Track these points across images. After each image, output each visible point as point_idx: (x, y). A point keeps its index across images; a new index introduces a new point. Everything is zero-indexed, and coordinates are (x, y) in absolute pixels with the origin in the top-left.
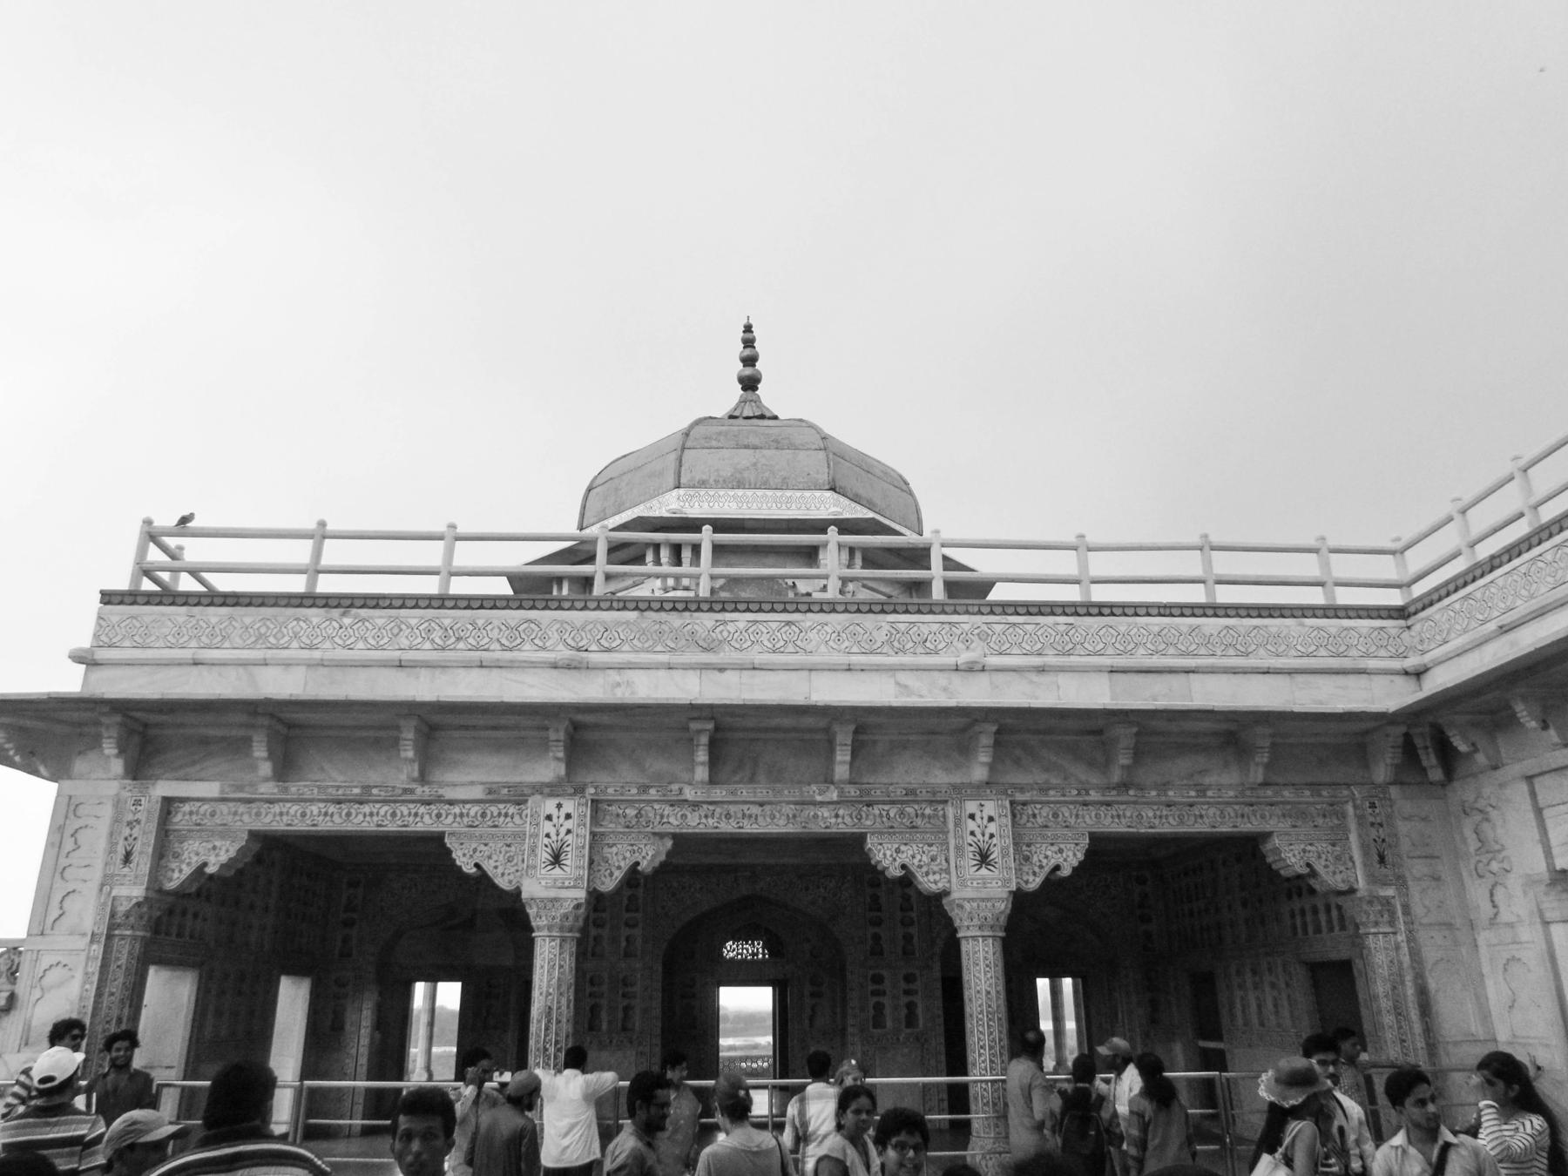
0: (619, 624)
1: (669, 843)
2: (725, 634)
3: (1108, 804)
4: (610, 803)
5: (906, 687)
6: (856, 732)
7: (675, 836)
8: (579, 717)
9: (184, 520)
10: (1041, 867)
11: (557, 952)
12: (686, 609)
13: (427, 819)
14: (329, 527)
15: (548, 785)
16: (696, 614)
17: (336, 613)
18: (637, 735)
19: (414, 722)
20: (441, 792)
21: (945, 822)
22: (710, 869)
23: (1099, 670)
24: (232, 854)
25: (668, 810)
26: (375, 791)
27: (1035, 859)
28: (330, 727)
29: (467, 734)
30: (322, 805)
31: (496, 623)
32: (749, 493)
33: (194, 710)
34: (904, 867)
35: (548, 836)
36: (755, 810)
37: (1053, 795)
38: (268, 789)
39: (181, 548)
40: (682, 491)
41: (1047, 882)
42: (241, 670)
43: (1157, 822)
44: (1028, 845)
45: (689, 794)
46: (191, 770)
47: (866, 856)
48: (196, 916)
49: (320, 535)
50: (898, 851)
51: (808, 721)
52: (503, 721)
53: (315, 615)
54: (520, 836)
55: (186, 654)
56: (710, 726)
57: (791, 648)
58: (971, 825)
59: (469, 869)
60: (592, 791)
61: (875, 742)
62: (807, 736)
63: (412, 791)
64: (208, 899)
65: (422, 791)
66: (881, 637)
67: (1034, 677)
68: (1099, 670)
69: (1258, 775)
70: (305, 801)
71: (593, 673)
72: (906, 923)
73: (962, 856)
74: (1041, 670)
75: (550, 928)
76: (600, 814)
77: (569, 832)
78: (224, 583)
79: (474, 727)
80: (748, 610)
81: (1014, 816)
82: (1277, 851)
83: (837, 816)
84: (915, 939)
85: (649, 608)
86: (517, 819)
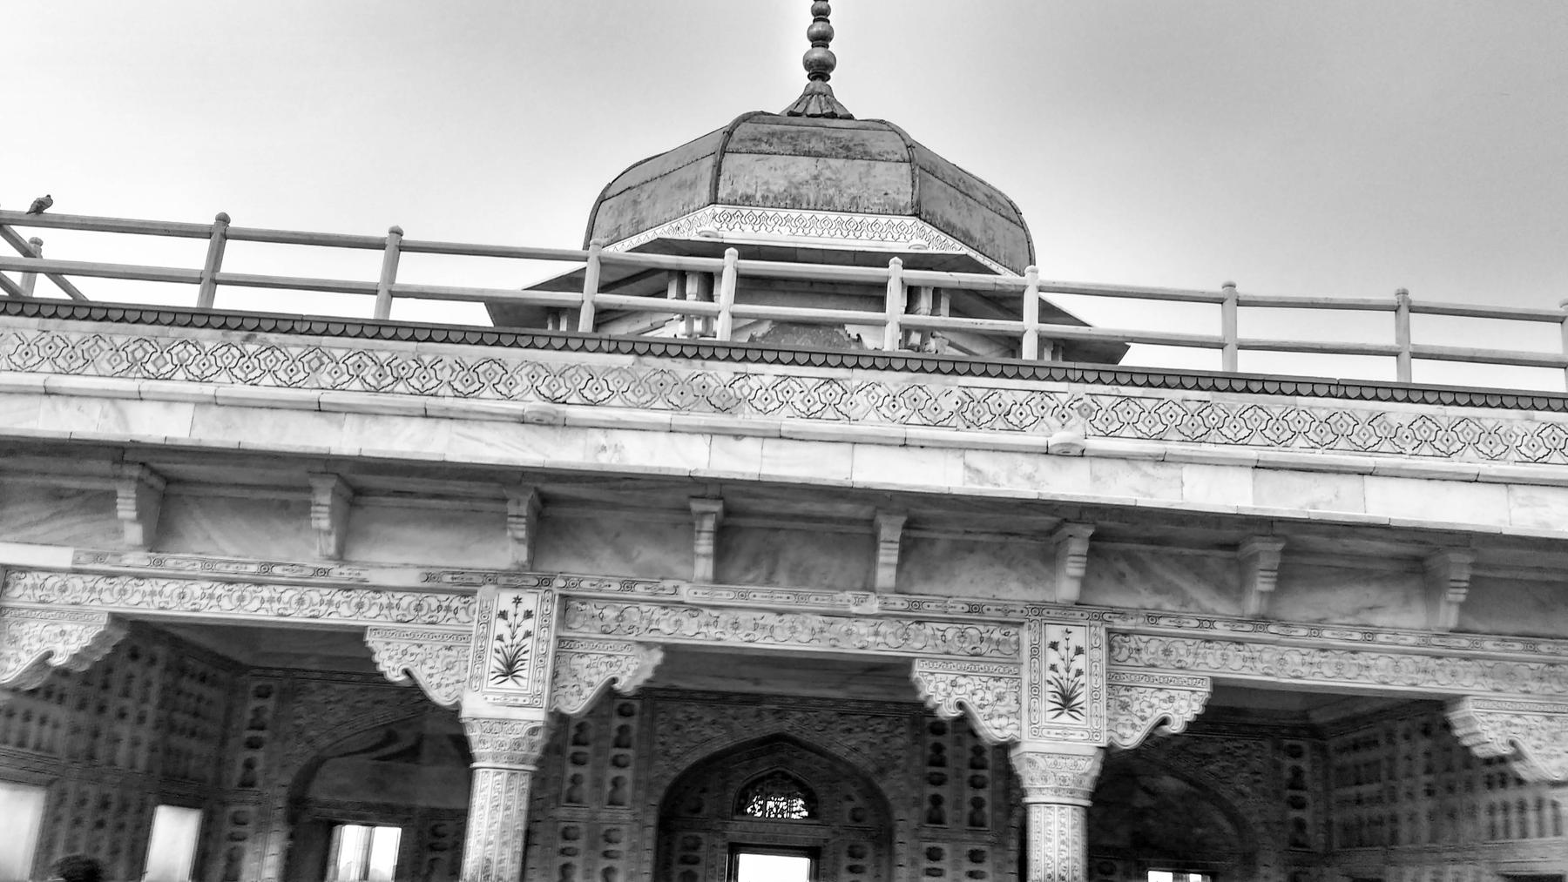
0: (611, 370)
1: (657, 657)
2: (746, 391)
3: (1239, 642)
4: (584, 600)
5: (978, 471)
6: (908, 526)
7: (668, 649)
8: (550, 488)
9: (40, 206)
10: (1143, 719)
11: (503, 788)
12: (697, 356)
13: (344, 610)
14: (234, 224)
15: (506, 573)
16: (709, 363)
17: (236, 337)
18: (624, 514)
19: (332, 482)
20: (364, 575)
21: (1018, 651)
22: (725, 697)
23: (1240, 464)
24: (86, 641)
25: (658, 613)
26: (277, 570)
27: (1136, 707)
28: (219, 485)
29: (406, 501)
30: (208, 585)
31: (448, 360)
32: (807, 215)
33: (42, 453)
34: (960, 705)
35: (500, 638)
36: (771, 619)
37: (1164, 625)
38: (137, 560)
39: (38, 242)
40: (719, 209)
41: (1150, 736)
42: (107, 404)
43: (1305, 670)
44: (1128, 688)
45: (687, 594)
46: (39, 530)
47: (913, 688)
48: (43, 721)
49: (220, 233)
50: (954, 684)
51: (845, 509)
52: (452, 486)
53: (209, 338)
54: (464, 637)
55: (36, 380)
56: (717, 507)
57: (830, 413)
58: (1053, 657)
59: (395, 676)
60: (561, 583)
61: (932, 542)
62: (845, 529)
63: (326, 572)
64: (61, 699)
65: (339, 573)
66: (948, 404)
67: (1148, 468)
68: (1240, 464)
69: (1449, 617)
70: (185, 578)
71: (571, 432)
72: (976, 784)
73: (1037, 696)
74: (1161, 460)
75: (495, 757)
76: (571, 615)
77: (528, 634)
78: (95, 290)
79: (411, 494)
80: (778, 361)
81: (1111, 648)
82: (1468, 720)
83: (876, 634)
84: (987, 810)
85: (649, 352)
86: (462, 615)
